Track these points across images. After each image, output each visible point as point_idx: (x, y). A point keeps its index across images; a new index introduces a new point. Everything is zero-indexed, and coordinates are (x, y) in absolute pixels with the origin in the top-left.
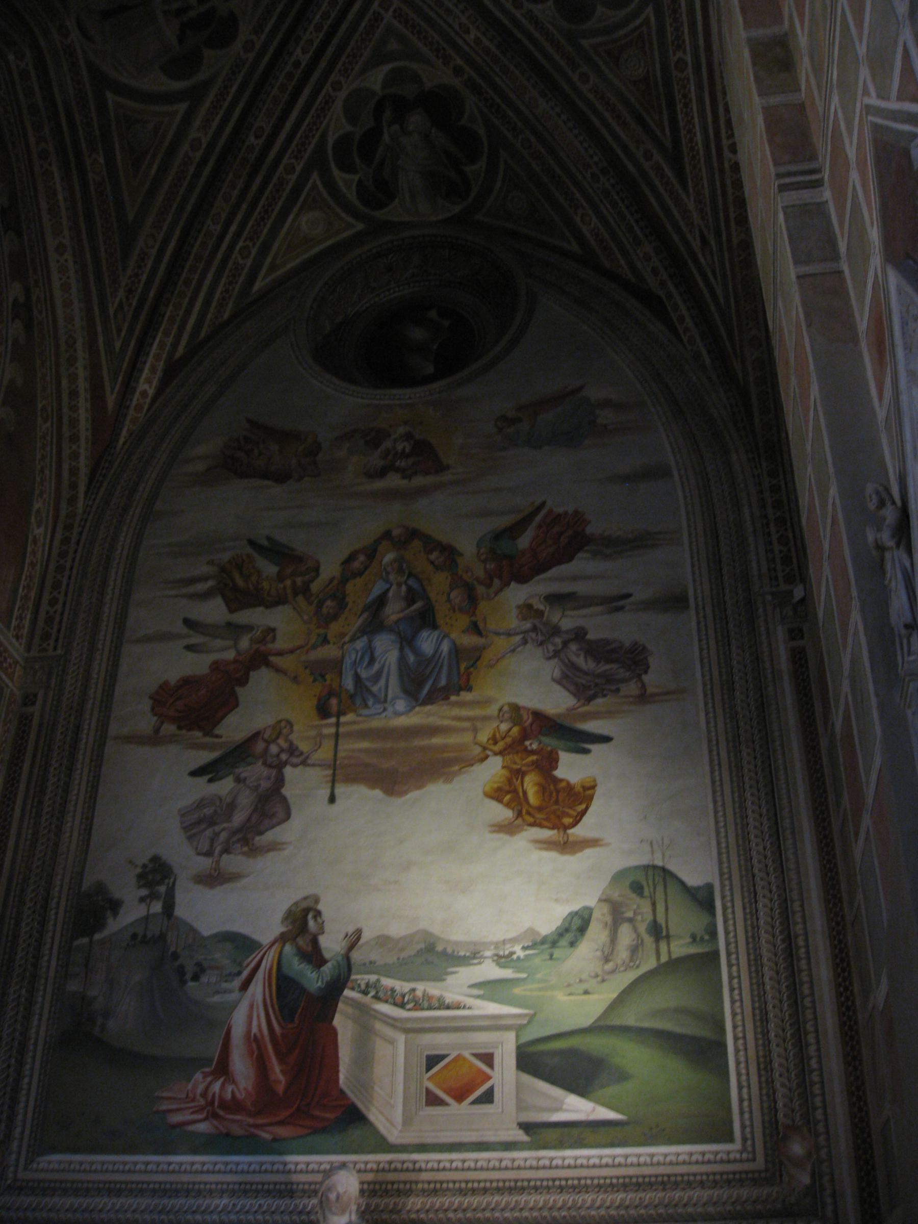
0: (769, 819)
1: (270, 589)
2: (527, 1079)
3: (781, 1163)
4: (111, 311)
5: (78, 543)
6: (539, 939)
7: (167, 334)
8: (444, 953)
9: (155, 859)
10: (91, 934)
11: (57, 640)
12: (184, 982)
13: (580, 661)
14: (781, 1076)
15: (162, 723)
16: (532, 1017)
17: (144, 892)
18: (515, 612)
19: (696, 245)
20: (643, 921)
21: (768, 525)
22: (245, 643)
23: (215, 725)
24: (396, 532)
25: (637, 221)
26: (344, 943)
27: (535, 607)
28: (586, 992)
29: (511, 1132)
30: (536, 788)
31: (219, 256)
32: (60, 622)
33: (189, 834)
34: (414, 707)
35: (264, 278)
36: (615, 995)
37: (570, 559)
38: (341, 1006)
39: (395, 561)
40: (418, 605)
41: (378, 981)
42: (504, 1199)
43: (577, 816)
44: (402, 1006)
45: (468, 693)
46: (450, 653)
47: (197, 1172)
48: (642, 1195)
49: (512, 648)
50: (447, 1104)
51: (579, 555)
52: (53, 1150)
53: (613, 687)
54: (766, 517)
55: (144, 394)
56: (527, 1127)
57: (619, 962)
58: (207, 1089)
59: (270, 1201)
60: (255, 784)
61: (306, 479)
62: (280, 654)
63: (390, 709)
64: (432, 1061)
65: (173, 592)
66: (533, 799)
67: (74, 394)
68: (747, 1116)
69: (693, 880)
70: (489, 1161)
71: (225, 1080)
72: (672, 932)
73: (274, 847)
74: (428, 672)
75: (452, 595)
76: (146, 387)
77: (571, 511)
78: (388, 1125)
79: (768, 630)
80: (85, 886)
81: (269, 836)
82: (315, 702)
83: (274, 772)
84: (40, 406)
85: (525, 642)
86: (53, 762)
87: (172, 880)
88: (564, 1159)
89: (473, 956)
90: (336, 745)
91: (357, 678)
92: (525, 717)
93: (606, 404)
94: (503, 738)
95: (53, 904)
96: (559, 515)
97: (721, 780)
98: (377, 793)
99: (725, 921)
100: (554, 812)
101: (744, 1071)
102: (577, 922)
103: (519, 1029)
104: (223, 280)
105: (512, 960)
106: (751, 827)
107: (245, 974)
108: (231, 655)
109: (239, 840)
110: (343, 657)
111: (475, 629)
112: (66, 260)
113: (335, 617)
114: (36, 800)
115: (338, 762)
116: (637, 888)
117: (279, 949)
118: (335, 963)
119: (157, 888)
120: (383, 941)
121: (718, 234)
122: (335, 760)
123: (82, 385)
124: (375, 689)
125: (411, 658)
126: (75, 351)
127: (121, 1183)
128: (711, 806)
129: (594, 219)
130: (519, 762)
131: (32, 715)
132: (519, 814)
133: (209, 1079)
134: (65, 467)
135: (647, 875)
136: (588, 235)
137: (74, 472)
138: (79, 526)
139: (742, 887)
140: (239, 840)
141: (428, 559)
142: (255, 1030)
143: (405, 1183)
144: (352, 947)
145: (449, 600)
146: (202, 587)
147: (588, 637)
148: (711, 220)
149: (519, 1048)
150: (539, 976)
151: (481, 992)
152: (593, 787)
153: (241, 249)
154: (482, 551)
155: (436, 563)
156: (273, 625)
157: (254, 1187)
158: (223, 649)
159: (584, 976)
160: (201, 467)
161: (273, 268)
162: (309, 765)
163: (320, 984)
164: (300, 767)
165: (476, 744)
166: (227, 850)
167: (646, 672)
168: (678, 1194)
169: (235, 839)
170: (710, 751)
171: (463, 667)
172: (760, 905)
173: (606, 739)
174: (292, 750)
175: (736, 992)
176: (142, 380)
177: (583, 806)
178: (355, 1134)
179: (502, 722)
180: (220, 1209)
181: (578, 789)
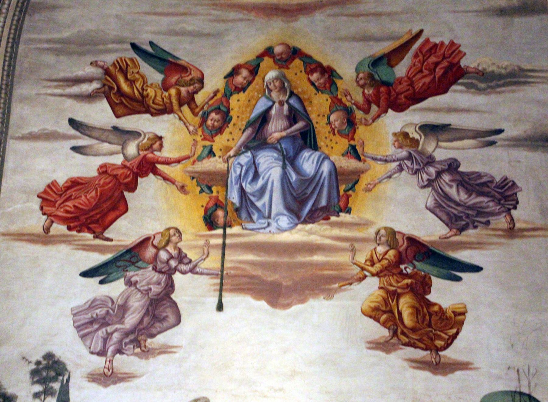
1: (156, 96)
9: (49, 356)
13: (453, 192)
15: (52, 222)
17: (38, 388)
18: (391, 139)
22: (132, 149)
23: (106, 227)
24: (278, 49)
27: (411, 136)
30: (410, 310)
33: (82, 333)
37: (445, 91)
39: (277, 78)
40: (300, 125)
43: (448, 339)
45: (347, 215)
49: (388, 174)
51: (454, 87)
53: (483, 220)
60: (146, 288)
62: (168, 162)
63: (274, 225)
65: (58, 91)
66: (408, 320)
73: (165, 350)
74: (309, 191)
75: (333, 118)
77: (447, 42)
81: (161, 339)
83: (163, 278)
85: (401, 169)
87: (66, 377)
90: (223, 254)
91: (242, 192)
92: (401, 242)
94: (380, 261)
96: (436, 45)
98: (263, 304)
100: (427, 334)
108: (118, 160)
109: (131, 342)
110: (228, 170)
113: (220, 130)
115: (225, 272)
122: (222, 271)
124: (259, 204)
125: (294, 177)
130: (395, 284)
132: (395, 334)
140: (131, 342)
141: (309, 79)
145: (329, 123)
146: (87, 88)
147: (461, 169)
152: (463, 314)
154: (361, 75)
155: (316, 84)
156: (159, 134)
158: (112, 154)
162: (197, 273)
164: (190, 274)
165: (355, 264)
166: (119, 351)
167: (515, 208)
169: (127, 340)
171: (342, 188)
173: (477, 269)
174: (181, 258)
177: (454, 331)
179: (379, 245)
181: (450, 314)
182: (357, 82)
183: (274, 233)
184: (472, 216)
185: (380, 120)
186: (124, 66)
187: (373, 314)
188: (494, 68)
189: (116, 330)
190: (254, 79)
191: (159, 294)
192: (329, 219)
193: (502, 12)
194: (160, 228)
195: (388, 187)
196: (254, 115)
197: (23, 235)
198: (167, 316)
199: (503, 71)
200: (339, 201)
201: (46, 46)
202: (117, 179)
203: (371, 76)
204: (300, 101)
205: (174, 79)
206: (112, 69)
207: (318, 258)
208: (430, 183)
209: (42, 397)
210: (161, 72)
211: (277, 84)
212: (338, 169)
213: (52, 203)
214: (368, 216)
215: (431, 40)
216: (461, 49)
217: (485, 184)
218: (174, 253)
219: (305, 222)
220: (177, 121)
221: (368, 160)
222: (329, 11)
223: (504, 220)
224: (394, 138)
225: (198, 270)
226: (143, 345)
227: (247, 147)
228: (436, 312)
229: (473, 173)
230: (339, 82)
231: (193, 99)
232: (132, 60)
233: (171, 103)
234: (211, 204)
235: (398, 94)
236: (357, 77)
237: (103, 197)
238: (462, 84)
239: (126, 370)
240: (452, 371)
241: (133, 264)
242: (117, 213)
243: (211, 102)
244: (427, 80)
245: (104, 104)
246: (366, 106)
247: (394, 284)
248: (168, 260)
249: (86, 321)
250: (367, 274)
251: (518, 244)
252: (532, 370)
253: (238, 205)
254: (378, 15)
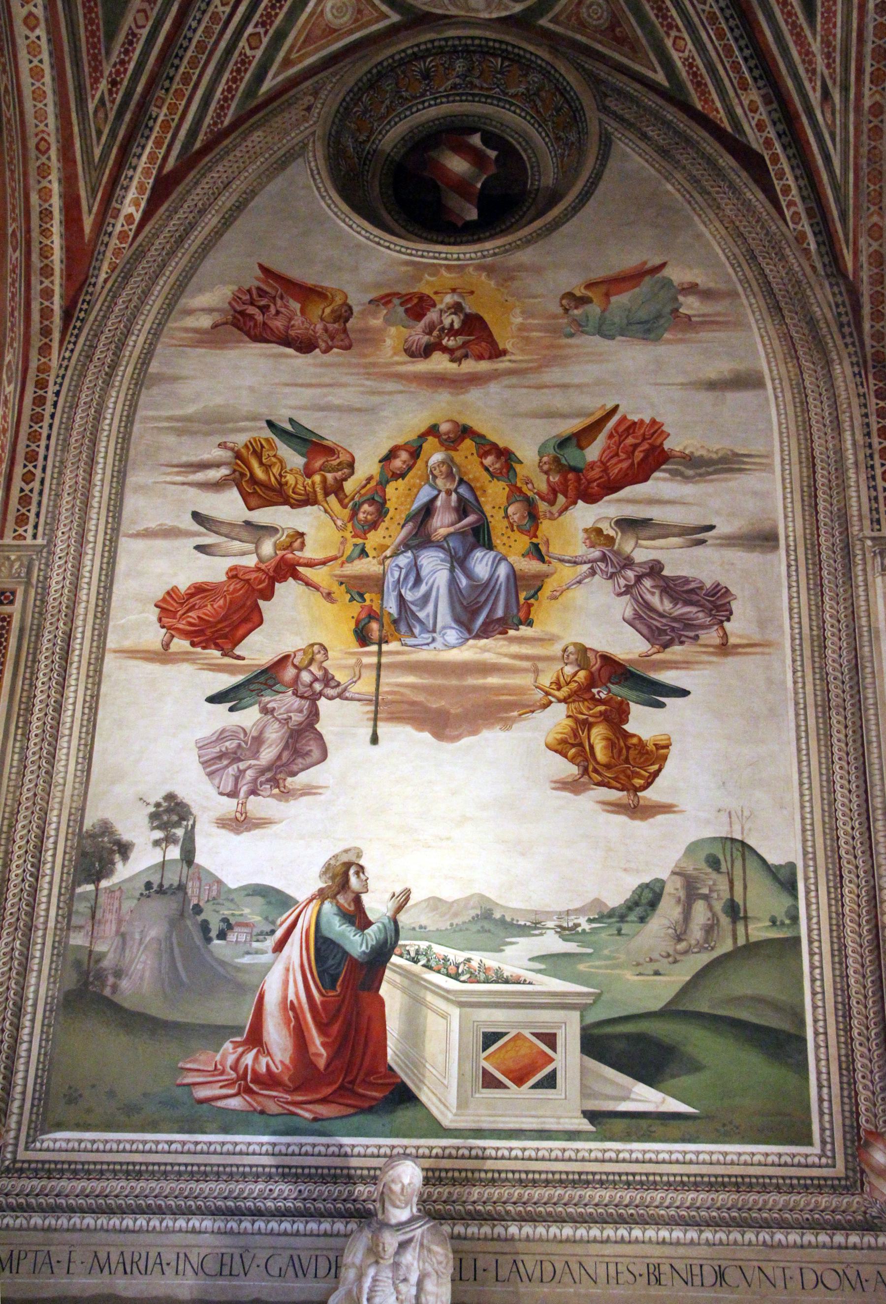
0: (858, 796)
1: (296, 483)
2: (593, 1064)
3: (863, 1172)
4: (91, 107)
5: (55, 405)
6: (606, 912)
7: (158, 144)
8: (502, 922)
9: (170, 797)
10: (97, 880)
11: (36, 527)
12: (209, 940)
13: (654, 600)
14: (863, 1077)
15: (173, 636)
16: (598, 996)
17: (159, 834)
18: (581, 536)
19: (815, 98)
20: (719, 898)
21: (871, 456)
22: (267, 548)
24: (444, 427)
25: (746, 59)
26: (390, 904)
28: (657, 973)
29: (577, 1121)
30: (604, 743)
31: (223, 45)
32: (39, 504)
33: (208, 770)
34: (468, 639)
35: (274, 77)
36: (688, 978)
37: (646, 479)
38: (388, 973)
39: (443, 463)
40: (471, 519)
41: (429, 947)
42: (569, 1193)
44: (456, 977)
46: (508, 578)
47: (228, 1153)
48: (714, 1195)
50: (506, 1087)
51: (656, 474)
52: (59, 1126)
53: (692, 634)
54: (870, 446)
55: (130, 218)
56: (592, 1116)
57: (693, 942)
58: (238, 1060)
59: (311, 1187)
60: (285, 716)
61: (335, 350)
62: (310, 564)
63: (439, 639)
64: (490, 1039)
66: (601, 754)
67: (46, 214)
68: (827, 1118)
69: (773, 859)
70: (551, 1150)
71: (258, 1051)
72: (749, 915)
73: (309, 791)
74: (483, 598)
75: (511, 510)
76: (132, 210)
77: (647, 421)
78: (441, 1107)
79: (865, 580)
80: (88, 825)
81: (302, 778)
82: (353, 625)
83: (306, 704)
84: (10, 230)
85: (593, 573)
86: (41, 675)
87: (191, 822)
88: (631, 1152)
89: (533, 927)
90: (379, 676)
91: (401, 599)
92: (593, 661)
93: (691, 289)
94: (568, 684)
95: (49, 843)
96: (634, 424)
97: (808, 749)
98: (426, 736)
99: (808, 905)
100: (623, 771)
101: (824, 1070)
102: (648, 895)
103: (583, 1009)
104: (226, 75)
105: (578, 933)
106: (838, 805)
107: (279, 933)
108: (251, 561)
109: (268, 781)
110: (384, 574)
111: (537, 553)
112: (38, 38)
113: (374, 525)
114: (21, 719)
116: (714, 863)
117: (317, 909)
118: (380, 925)
119: (173, 830)
120: (435, 904)
121: (845, 89)
122: (377, 698)
123: (56, 202)
124: (421, 615)
125: (464, 582)
126: (49, 159)
127: (141, 1164)
128: (796, 776)
129: (690, 45)
131: (10, 616)
132: (585, 771)
133: (240, 1050)
134: (35, 307)
135: (724, 850)
136: (679, 64)
137: (46, 313)
138: (55, 383)
139: (827, 869)
140: (268, 781)
141: (482, 463)
142: (291, 996)
143: (460, 1171)
144: (400, 909)
145: (507, 516)
146: (214, 475)
147: (665, 573)
148: (838, 70)
149: (583, 1029)
150: (606, 952)
151: (543, 967)
152: (667, 747)
153: (250, 35)
154: (545, 459)
156: (301, 530)
157: (293, 1170)
158: (243, 554)
159: (655, 956)
160: (205, 322)
161: (287, 63)
162: (347, 699)
163: (364, 948)
166: (254, 792)
167: (728, 620)
168: (752, 1197)
169: (263, 779)
170: (797, 715)
171: (522, 596)
172: (846, 891)
173: (684, 693)
174: (327, 680)
175: (818, 983)
176: (127, 201)
177: (656, 767)
178: (404, 1115)
180: (255, 1195)
181: (651, 747)
182: (540, 467)
183: (439, 650)
184: (679, 629)
185: (568, 513)
186: (258, 449)
187: (559, 747)
188: (703, 452)
189: (249, 767)
190: (415, 464)
191: (301, 724)
192: (506, 633)
193: (712, 385)
194: (303, 645)
195: (578, 595)
196: (416, 505)
197: (138, 652)
198: (311, 751)
199: (714, 456)
200: (519, 610)
201: (166, 424)
202: (250, 584)
203: (556, 460)
204: (472, 489)
205: (318, 464)
206: (243, 451)
207: (493, 680)
208: (628, 590)
209: (164, 845)
210: (302, 455)
211: (444, 468)
212: (518, 573)
213: (172, 614)
214: (554, 629)
215: (629, 417)
216: (664, 428)
217: (692, 591)
218: (319, 674)
219: (478, 637)
220: (322, 514)
221: (554, 561)
222: (506, 381)
223: (715, 634)
224: (585, 536)
225: (347, 694)
226: (282, 785)
227: (407, 545)
228: (634, 745)
229: (679, 577)
230: (518, 467)
231: (341, 488)
232: (267, 440)
233: (315, 492)
234: (363, 616)
235: (590, 482)
236: (540, 461)
237: (233, 606)
238: (665, 471)
239: (263, 815)
240: (653, 815)
241: (270, 687)
242: (249, 625)
243: (363, 492)
244: (625, 465)
245: (234, 494)
246: (551, 497)
247: (585, 711)
248: (312, 683)
249: (215, 755)
250: (553, 699)
251: (731, 662)
252: (746, 813)
253: (396, 616)
254: (565, 386)
